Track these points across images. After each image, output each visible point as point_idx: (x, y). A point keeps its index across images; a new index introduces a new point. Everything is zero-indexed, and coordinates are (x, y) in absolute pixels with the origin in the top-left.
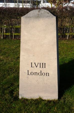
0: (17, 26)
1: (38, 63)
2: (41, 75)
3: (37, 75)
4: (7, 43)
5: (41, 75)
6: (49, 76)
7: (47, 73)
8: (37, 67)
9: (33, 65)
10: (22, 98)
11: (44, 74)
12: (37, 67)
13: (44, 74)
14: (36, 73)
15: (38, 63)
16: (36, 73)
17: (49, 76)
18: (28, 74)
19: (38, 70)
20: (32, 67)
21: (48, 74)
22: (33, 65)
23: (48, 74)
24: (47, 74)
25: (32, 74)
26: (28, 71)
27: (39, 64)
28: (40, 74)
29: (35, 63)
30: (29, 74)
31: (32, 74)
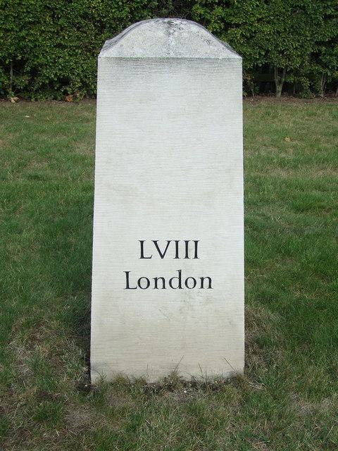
0: (81, 149)
1: (169, 242)
2: (180, 287)
3: (164, 287)
4: (26, 370)
5: (180, 287)
6: (210, 287)
7: (202, 279)
8: (162, 257)
9: (150, 249)
10: (102, 381)
11: (191, 282)
12: (162, 257)
13: (191, 282)
14: (160, 282)
15: (169, 242)
16: (160, 282)
17: (210, 287)
18: (128, 287)
19: (167, 267)
20: (142, 257)
21: (206, 282)
22: (150, 249)
23: (206, 282)
24: (206, 282)
25: (144, 283)
26: (127, 273)
27: (173, 245)
28: (175, 283)
29: (155, 242)
30: (133, 283)
31: (144, 283)
